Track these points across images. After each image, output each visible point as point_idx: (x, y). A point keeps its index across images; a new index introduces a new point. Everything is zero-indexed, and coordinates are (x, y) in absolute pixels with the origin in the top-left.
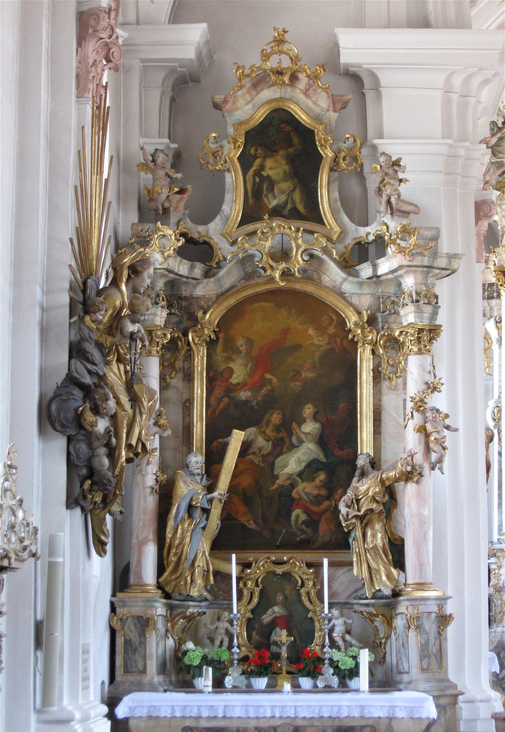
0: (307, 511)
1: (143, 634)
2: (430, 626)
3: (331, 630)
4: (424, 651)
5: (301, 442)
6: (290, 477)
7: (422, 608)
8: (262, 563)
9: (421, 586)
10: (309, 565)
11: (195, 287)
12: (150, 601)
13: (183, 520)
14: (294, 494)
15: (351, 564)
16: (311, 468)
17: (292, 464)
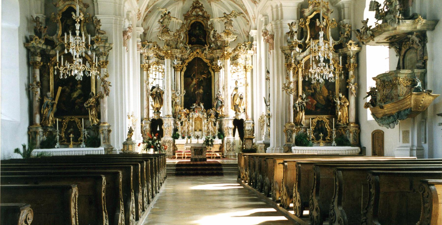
0: (79, 106)
1: (35, 136)
2: (106, 132)
3: (84, 134)
4: (104, 138)
5: (77, 90)
6: (75, 98)
7: (103, 128)
8: (67, 119)
9: (104, 123)
10: (79, 119)
11: (50, 52)
12: (37, 128)
13: (46, 108)
14: (76, 102)
15: (89, 119)
16: (79, 96)
17: (75, 95)
